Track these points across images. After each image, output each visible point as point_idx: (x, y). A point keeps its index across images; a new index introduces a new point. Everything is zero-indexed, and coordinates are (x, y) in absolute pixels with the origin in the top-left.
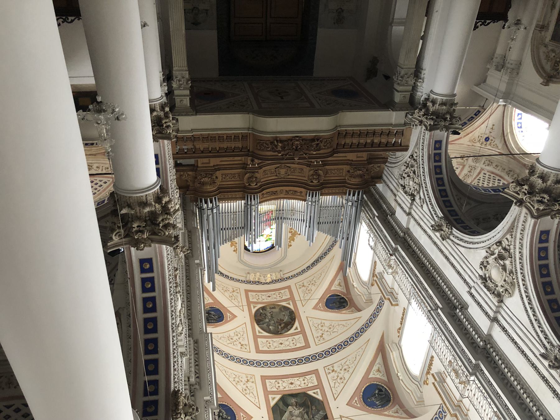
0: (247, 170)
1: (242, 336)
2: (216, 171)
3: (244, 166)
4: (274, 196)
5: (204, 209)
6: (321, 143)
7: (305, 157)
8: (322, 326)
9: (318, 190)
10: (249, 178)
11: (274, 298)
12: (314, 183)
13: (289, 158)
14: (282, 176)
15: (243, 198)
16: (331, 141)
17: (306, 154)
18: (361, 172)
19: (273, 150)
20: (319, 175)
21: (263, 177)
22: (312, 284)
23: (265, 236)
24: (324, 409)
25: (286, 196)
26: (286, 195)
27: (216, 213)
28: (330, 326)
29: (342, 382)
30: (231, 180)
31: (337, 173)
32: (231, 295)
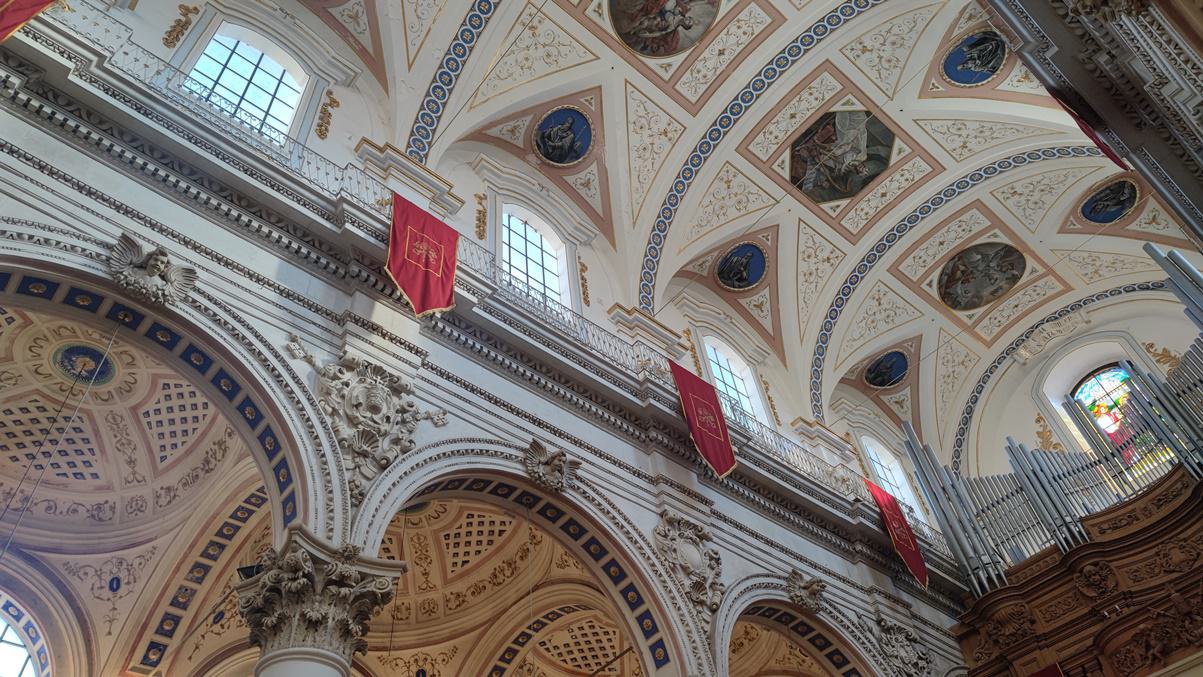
4: (1160, 495)
6: (1141, 655)
7: (1155, 608)
8: (888, 316)
9: (1069, 555)
11: (1005, 309)
13: (1193, 589)
16: (1122, 668)
17: (1159, 614)
18: (1007, 633)
20: (1089, 586)
22: (949, 376)
24: (809, 194)
25: (1130, 507)
26: (1134, 510)
28: (874, 324)
29: (804, 252)
31: (1053, 608)
32: (1098, 263)
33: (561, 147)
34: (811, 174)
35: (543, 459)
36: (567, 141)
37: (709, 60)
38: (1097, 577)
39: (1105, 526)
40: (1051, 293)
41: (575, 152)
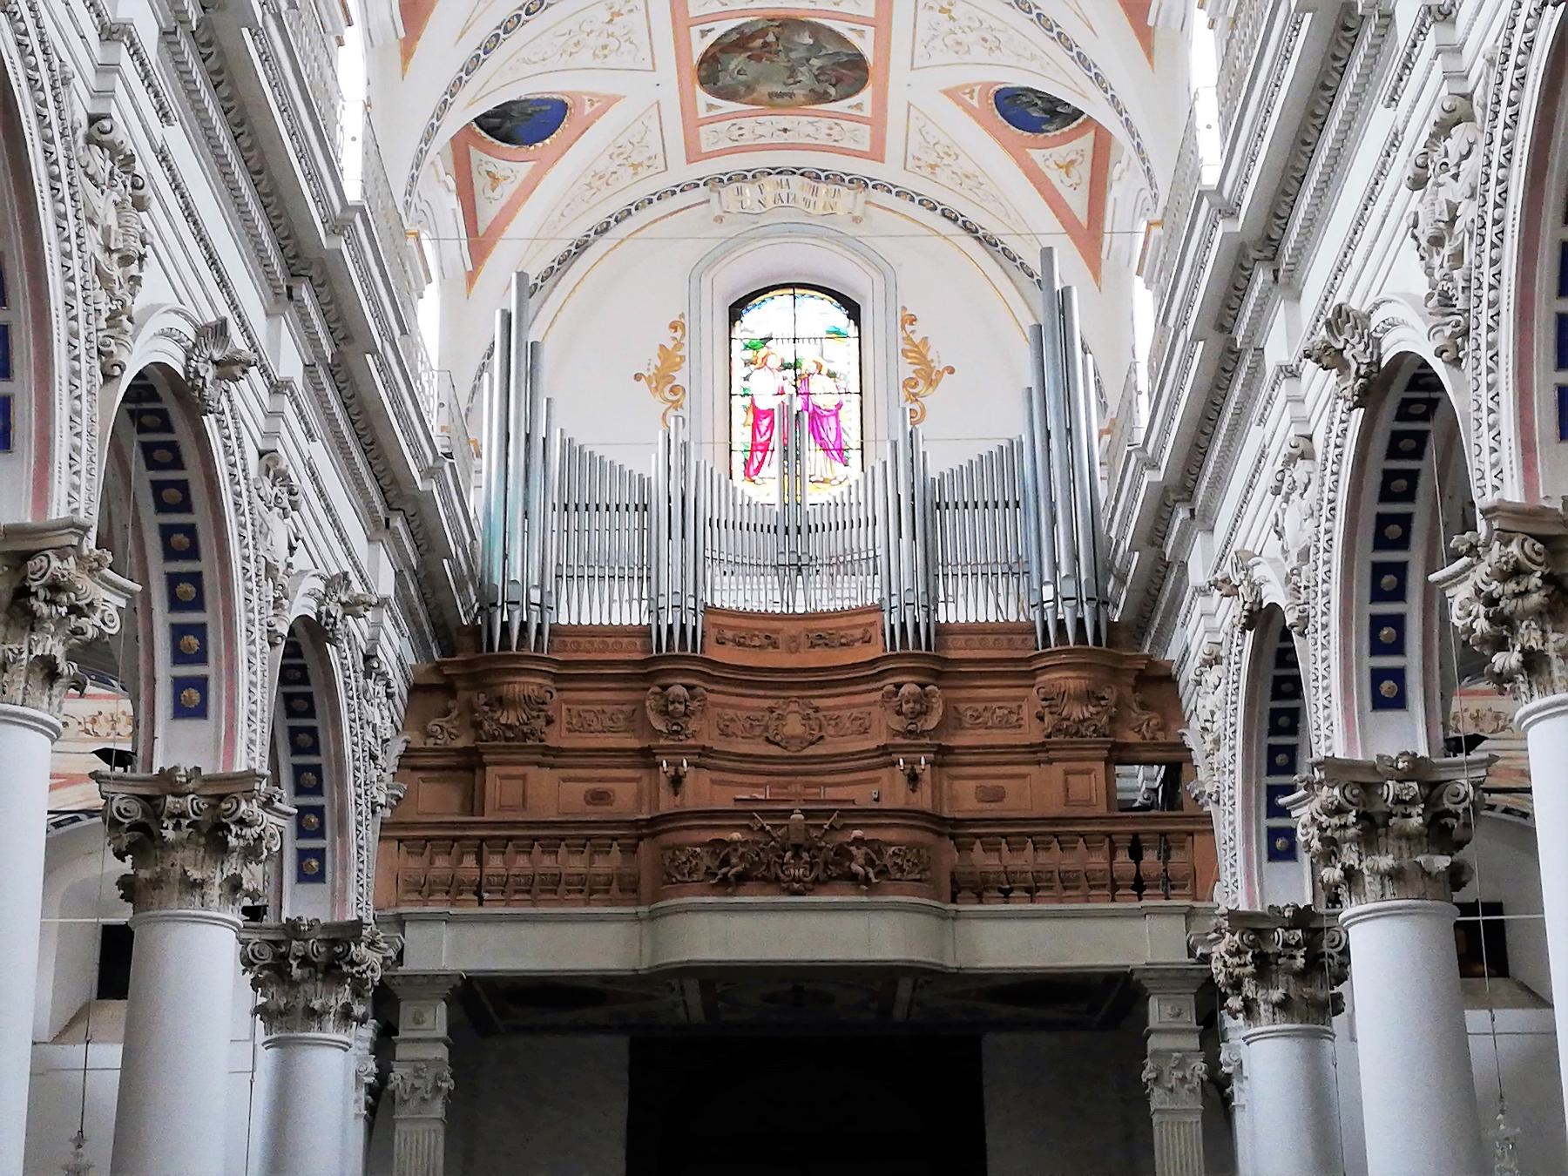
0: (932, 746)
1: (935, 36)
2: (1043, 744)
3: (943, 756)
4: (823, 630)
5: (1088, 599)
6: (708, 868)
8: (604, 47)
10: (924, 713)
11: (767, 126)
12: (683, 685)
14: (794, 707)
15: (944, 631)
16: (672, 872)
17: (762, 828)
18: (503, 721)
19: (877, 847)
20: (664, 713)
21: (868, 709)
23: (774, 362)
26: (777, 631)
27: (1042, 584)
30: (989, 705)
35: (217, 356)
38: (682, 708)
39: (729, 634)
40: (847, 144)
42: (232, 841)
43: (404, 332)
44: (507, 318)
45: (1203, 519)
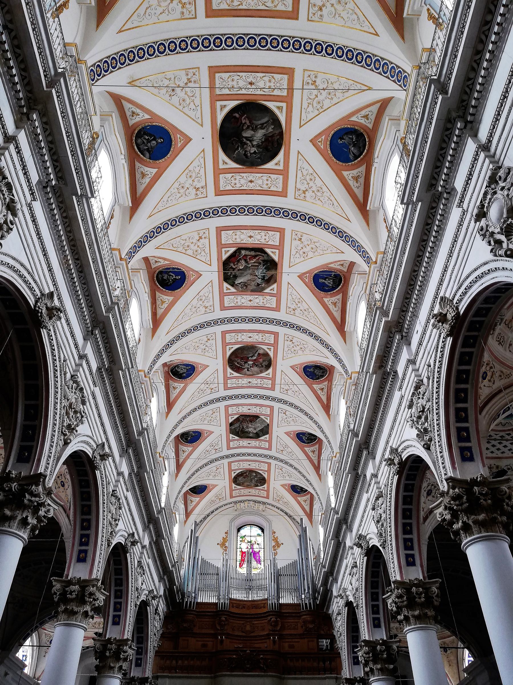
11: (246, 491)
14: (248, 623)
15: (281, 605)
23: (246, 541)
24: (230, 429)
25: (245, 603)
26: (245, 604)
27: (302, 594)
33: (178, 372)
34: (237, 425)
36: (181, 372)
37: (245, 381)
41: (181, 376)
42: (121, 656)
43: (170, 535)
44: (192, 531)
45: (336, 580)
